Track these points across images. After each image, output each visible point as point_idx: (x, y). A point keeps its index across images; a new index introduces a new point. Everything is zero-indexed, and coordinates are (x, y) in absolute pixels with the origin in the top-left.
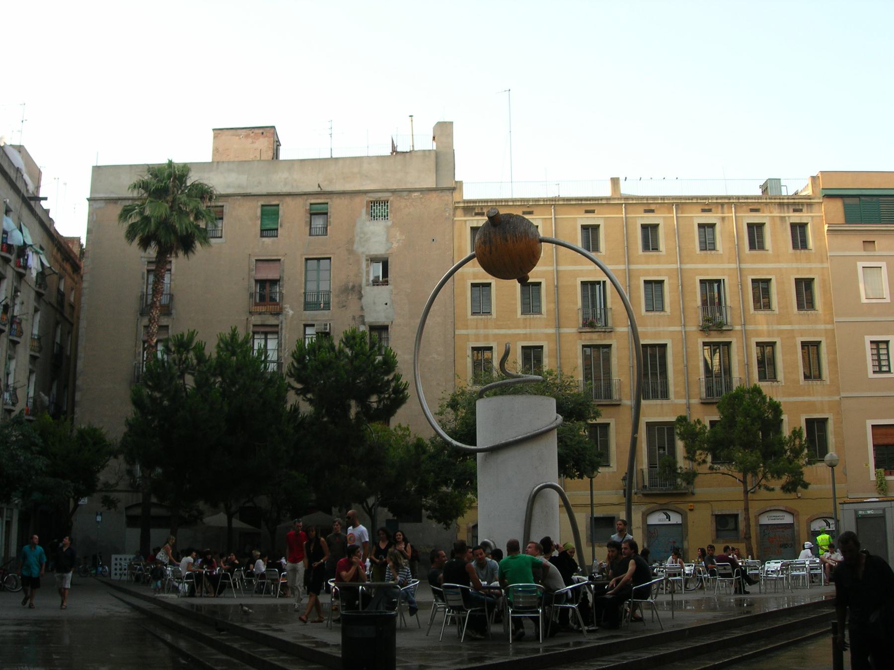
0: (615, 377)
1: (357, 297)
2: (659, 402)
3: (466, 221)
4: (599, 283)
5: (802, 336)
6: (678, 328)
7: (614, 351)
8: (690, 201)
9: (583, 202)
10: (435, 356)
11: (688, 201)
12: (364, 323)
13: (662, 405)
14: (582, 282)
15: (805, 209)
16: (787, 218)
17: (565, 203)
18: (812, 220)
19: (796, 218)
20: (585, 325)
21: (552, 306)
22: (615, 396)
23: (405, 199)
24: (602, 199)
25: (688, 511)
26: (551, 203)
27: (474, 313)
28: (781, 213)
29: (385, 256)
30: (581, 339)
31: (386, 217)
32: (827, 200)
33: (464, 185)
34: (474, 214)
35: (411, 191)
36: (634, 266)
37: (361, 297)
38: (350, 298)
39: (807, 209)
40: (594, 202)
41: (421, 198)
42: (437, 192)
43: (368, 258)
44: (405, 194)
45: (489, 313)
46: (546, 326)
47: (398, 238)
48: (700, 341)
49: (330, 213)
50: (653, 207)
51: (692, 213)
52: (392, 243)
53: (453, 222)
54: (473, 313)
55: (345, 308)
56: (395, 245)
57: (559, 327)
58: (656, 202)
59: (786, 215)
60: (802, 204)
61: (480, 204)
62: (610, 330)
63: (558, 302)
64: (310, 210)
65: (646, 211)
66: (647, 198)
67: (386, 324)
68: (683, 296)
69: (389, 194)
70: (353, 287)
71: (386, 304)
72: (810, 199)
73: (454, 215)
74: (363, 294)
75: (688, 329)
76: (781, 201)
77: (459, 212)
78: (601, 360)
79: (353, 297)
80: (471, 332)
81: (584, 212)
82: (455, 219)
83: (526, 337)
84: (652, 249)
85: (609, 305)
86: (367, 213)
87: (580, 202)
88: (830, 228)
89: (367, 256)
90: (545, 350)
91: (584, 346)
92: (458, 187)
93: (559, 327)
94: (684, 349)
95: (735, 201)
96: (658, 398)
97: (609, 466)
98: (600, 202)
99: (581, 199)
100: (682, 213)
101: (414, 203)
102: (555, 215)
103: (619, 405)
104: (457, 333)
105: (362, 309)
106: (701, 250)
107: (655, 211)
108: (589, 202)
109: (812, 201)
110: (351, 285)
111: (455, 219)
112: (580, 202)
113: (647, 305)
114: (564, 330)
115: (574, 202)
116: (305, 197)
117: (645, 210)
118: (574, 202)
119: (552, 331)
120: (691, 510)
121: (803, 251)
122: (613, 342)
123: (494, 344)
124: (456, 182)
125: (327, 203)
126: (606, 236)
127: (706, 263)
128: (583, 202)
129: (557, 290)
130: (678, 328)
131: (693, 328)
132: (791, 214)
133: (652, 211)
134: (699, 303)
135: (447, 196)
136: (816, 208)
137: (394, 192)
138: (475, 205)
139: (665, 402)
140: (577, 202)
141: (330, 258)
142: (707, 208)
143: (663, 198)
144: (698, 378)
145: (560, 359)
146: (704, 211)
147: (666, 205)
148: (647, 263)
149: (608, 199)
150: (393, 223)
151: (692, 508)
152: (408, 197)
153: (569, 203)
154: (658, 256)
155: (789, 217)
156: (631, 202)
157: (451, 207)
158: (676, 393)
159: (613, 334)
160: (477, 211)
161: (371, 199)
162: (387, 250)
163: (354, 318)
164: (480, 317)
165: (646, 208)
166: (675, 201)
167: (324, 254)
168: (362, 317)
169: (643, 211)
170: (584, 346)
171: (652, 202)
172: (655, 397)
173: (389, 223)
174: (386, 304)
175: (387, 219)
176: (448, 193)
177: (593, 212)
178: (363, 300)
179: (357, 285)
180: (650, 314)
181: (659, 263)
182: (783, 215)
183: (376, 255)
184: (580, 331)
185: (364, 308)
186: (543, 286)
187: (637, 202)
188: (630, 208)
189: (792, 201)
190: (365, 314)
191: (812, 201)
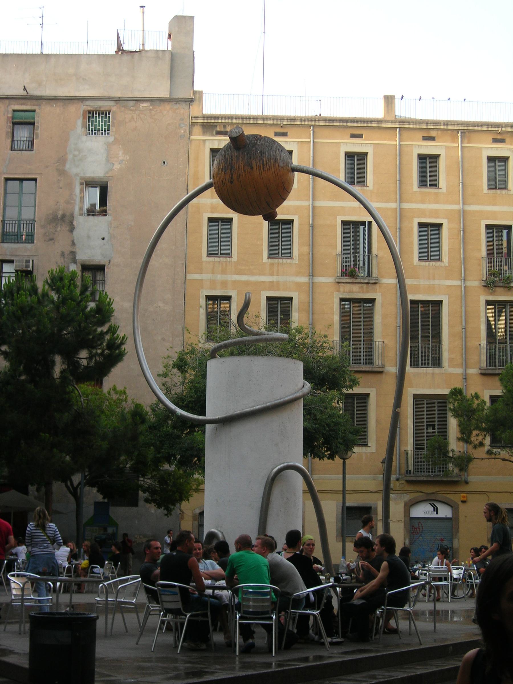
0: (378, 338)
1: (68, 228)
2: (430, 370)
3: (204, 141)
4: (363, 223)
6: (457, 283)
7: (378, 305)
8: (480, 128)
9: (349, 124)
10: (161, 304)
12: (75, 261)
13: (433, 374)
14: (343, 222)
17: (327, 124)
20: (344, 274)
21: (306, 249)
22: (378, 362)
23: (131, 110)
24: (371, 121)
25: (460, 503)
26: (310, 123)
27: (210, 254)
29: (105, 180)
30: (338, 291)
31: (106, 131)
33: (204, 95)
34: (215, 133)
35: (139, 100)
36: (406, 204)
37: (72, 229)
38: (59, 229)
40: (362, 125)
41: (151, 110)
42: (171, 103)
43: (83, 181)
44: (132, 103)
45: (229, 255)
46: (298, 274)
47: (121, 158)
48: (483, 298)
49: (38, 123)
50: (433, 134)
51: (481, 143)
52: (114, 164)
53: (189, 140)
54: (210, 255)
55: (51, 242)
56: (117, 167)
57: (312, 275)
58: (438, 127)
61: (223, 121)
62: (374, 281)
63: (313, 246)
64: (13, 118)
65: (425, 138)
66: (427, 122)
67: (102, 263)
68: (464, 243)
69: (112, 103)
70: (64, 216)
71: (103, 239)
73: (191, 133)
74: (75, 226)
75: (468, 283)
77: (197, 129)
78: (362, 317)
79: (62, 229)
80: (206, 277)
81: (349, 136)
82: (192, 137)
83: (272, 286)
84: (430, 185)
85: (374, 251)
86: (83, 125)
87: (345, 124)
89: (81, 178)
90: (295, 303)
91: (342, 300)
92: (197, 98)
93: (312, 275)
94: (463, 307)
96: (428, 365)
97: (366, 445)
98: (369, 125)
99: (346, 120)
100: (469, 143)
101: (142, 116)
102: (314, 138)
103: (381, 372)
104: (189, 277)
105: (73, 244)
106: (490, 188)
107: (436, 139)
108: (355, 125)
110: (60, 213)
111: (192, 137)
112: (345, 124)
113: (420, 252)
114: (319, 280)
115: (338, 124)
116: (7, 101)
117: (423, 137)
118: (338, 124)
119: (304, 279)
120: (464, 502)
122: (378, 297)
123: (233, 293)
124: (195, 92)
125: (34, 111)
126: (374, 166)
127: (495, 204)
128: (349, 124)
129: (313, 230)
130: (457, 283)
131: (474, 283)
133: (432, 139)
134: (484, 252)
135: (182, 109)
137: (118, 100)
138: (216, 121)
139: (437, 370)
140: (341, 124)
141: (35, 180)
142: (499, 137)
143: (446, 123)
144: (477, 344)
145: (313, 314)
146: (495, 141)
147: (449, 132)
148: (423, 202)
149: (379, 121)
150: (115, 138)
151: (465, 499)
152: (134, 108)
153: (332, 124)
154: (436, 194)
156: (407, 126)
157: (187, 123)
158: (451, 360)
159: (377, 286)
160: (218, 129)
161: (89, 109)
162: (107, 173)
163: (63, 254)
164: (217, 259)
165: (426, 135)
166: (461, 128)
167: (28, 174)
168: (73, 253)
169: (421, 138)
170: (342, 300)
171: (432, 127)
172: (425, 364)
173: (111, 139)
174: (103, 239)
175: (108, 134)
176: (184, 105)
177: (360, 136)
178: (75, 233)
179: (68, 214)
180: (423, 263)
181: (437, 202)
183: (93, 178)
184: (338, 280)
185: (76, 242)
186: (296, 224)
187: (415, 127)
188: (405, 134)
190: (77, 250)
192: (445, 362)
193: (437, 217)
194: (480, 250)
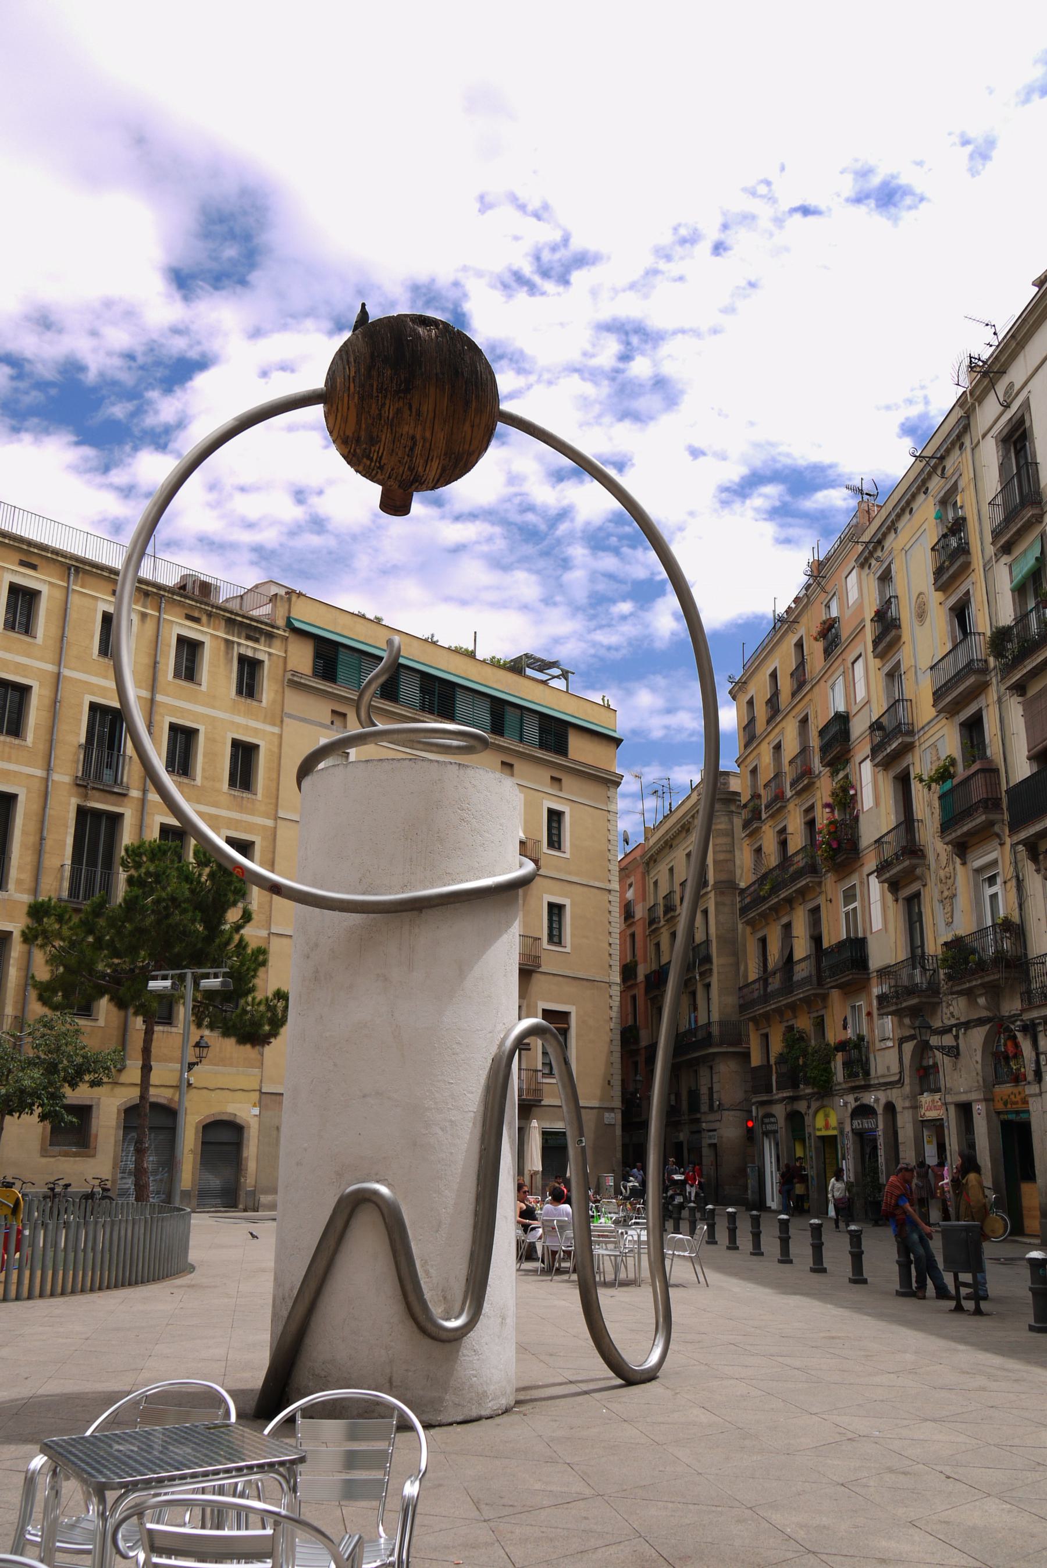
5: (229, 829)
8: (99, 572)
11: (94, 570)
15: (263, 639)
16: (236, 646)
18: (269, 660)
19: (248, 648)
28: (227, 633)
32: (293, 639)
39: (265, 641)
48: (74, 802)
50: (34, 561)
51: (97, 592)
58: (44, 553)
59: (236, 639)
60: (261, 631)
65: (23, 564)
66: (30, 543)
72: (273, 627)
76: (233, 617)
88: (295, 679)
95: (166, 594)
107: (38, 568)
109: (275, 631)
121: (249, 701)
131: (63, 776)
132: (243, 641)
133: (34, 567)
134: (83, 740)
136: (277, 643)
144: (59, 864)
154: (30, 644)
155: (239, 644)
158: (19, 882)
166: (74, 563)
169: (17, 561)
171: (36, 551)
181: (28, 656)
182: (231, 638)
189: (248, 622)
191: (275, 631)
192: (11, 885)
193: (25, 676)
194: (78, 734)
